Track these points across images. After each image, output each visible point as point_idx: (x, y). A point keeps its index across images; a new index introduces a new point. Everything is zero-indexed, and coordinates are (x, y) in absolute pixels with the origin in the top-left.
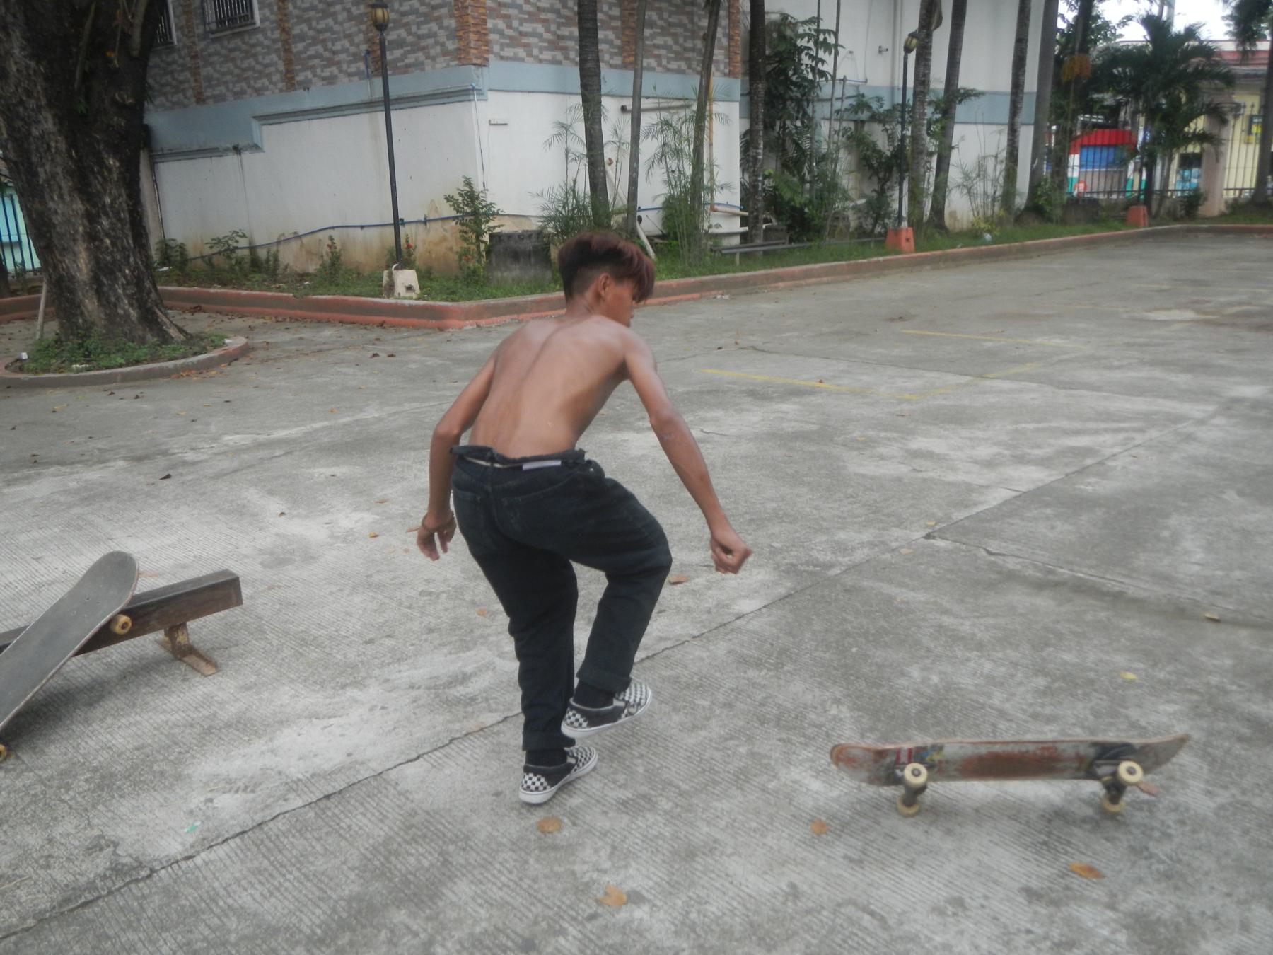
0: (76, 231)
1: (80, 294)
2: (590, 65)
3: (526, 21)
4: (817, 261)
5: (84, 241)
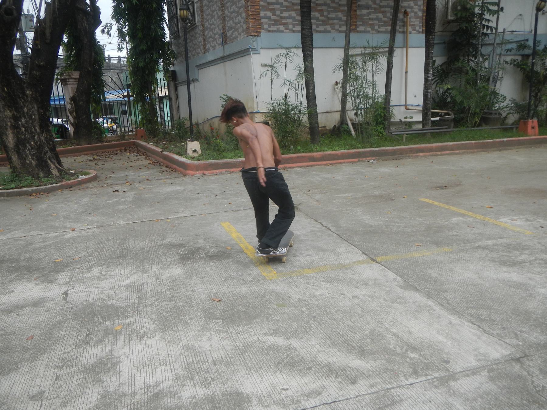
0: (7, 125)
1: (10, 153)
2: (305, 32)
3: (285, 11)
4: (454, 140)
5: (11, 129)
